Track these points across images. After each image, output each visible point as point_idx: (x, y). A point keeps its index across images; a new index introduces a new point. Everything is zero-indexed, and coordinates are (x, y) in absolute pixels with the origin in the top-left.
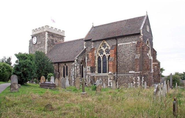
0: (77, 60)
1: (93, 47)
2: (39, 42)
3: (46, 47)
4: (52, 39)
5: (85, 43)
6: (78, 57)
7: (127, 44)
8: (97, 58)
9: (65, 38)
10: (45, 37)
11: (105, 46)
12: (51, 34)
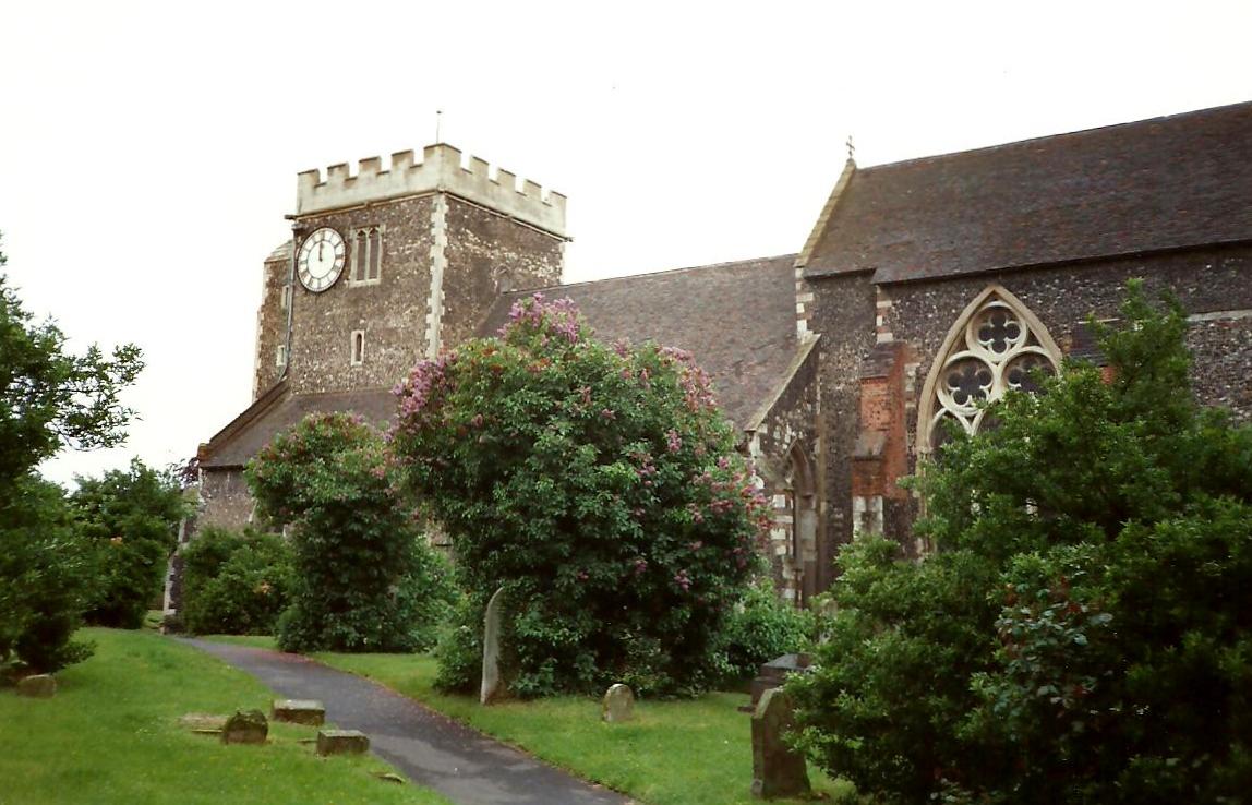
0: (762, 437)
1: (885, 337)
2: (360, 277)
3: (430, 318)
5: (810, 297)
6: (769, 421)
7: (1223, 323)
8: (926, 425)
9: (568, 250)
10: (423, 231)
11: (997, 328)
12: (471, 217)
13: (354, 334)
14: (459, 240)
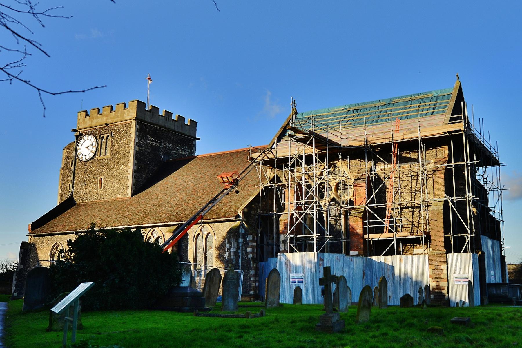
4: (152, 146)
13: (99, 178)
14: (144, 139)
